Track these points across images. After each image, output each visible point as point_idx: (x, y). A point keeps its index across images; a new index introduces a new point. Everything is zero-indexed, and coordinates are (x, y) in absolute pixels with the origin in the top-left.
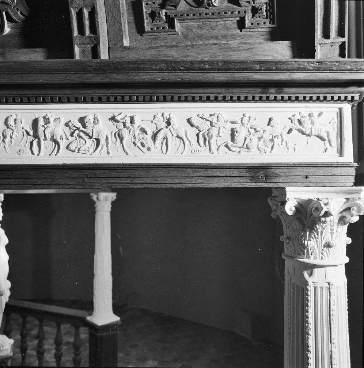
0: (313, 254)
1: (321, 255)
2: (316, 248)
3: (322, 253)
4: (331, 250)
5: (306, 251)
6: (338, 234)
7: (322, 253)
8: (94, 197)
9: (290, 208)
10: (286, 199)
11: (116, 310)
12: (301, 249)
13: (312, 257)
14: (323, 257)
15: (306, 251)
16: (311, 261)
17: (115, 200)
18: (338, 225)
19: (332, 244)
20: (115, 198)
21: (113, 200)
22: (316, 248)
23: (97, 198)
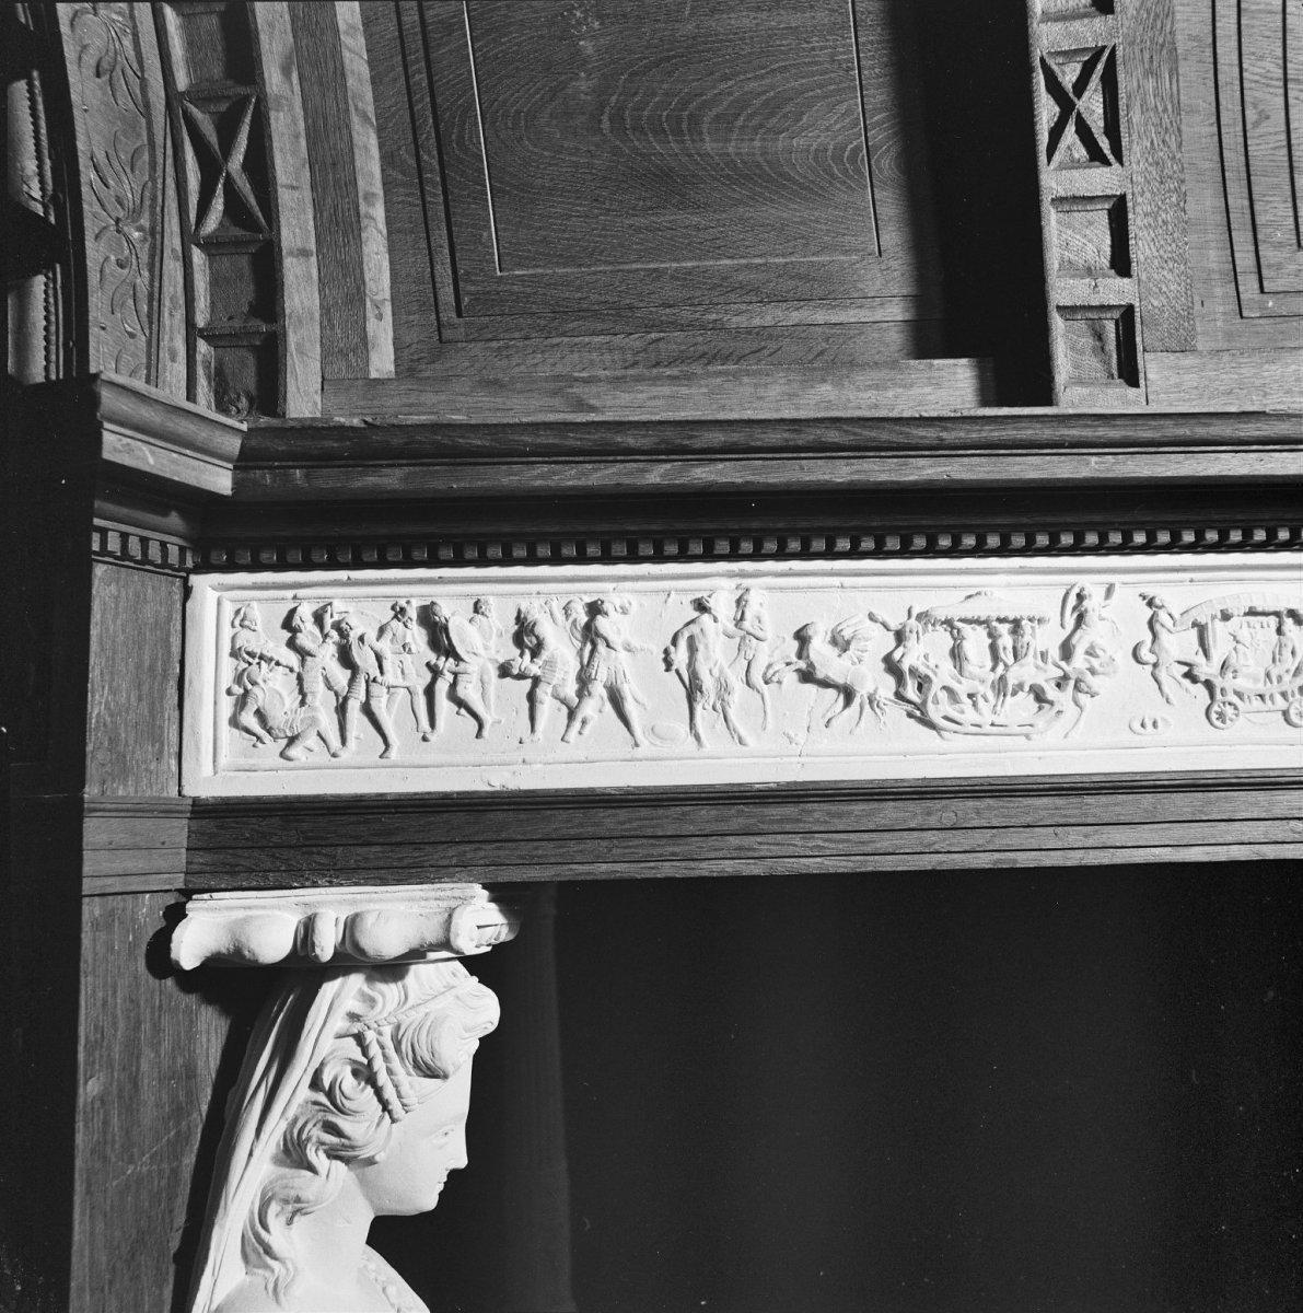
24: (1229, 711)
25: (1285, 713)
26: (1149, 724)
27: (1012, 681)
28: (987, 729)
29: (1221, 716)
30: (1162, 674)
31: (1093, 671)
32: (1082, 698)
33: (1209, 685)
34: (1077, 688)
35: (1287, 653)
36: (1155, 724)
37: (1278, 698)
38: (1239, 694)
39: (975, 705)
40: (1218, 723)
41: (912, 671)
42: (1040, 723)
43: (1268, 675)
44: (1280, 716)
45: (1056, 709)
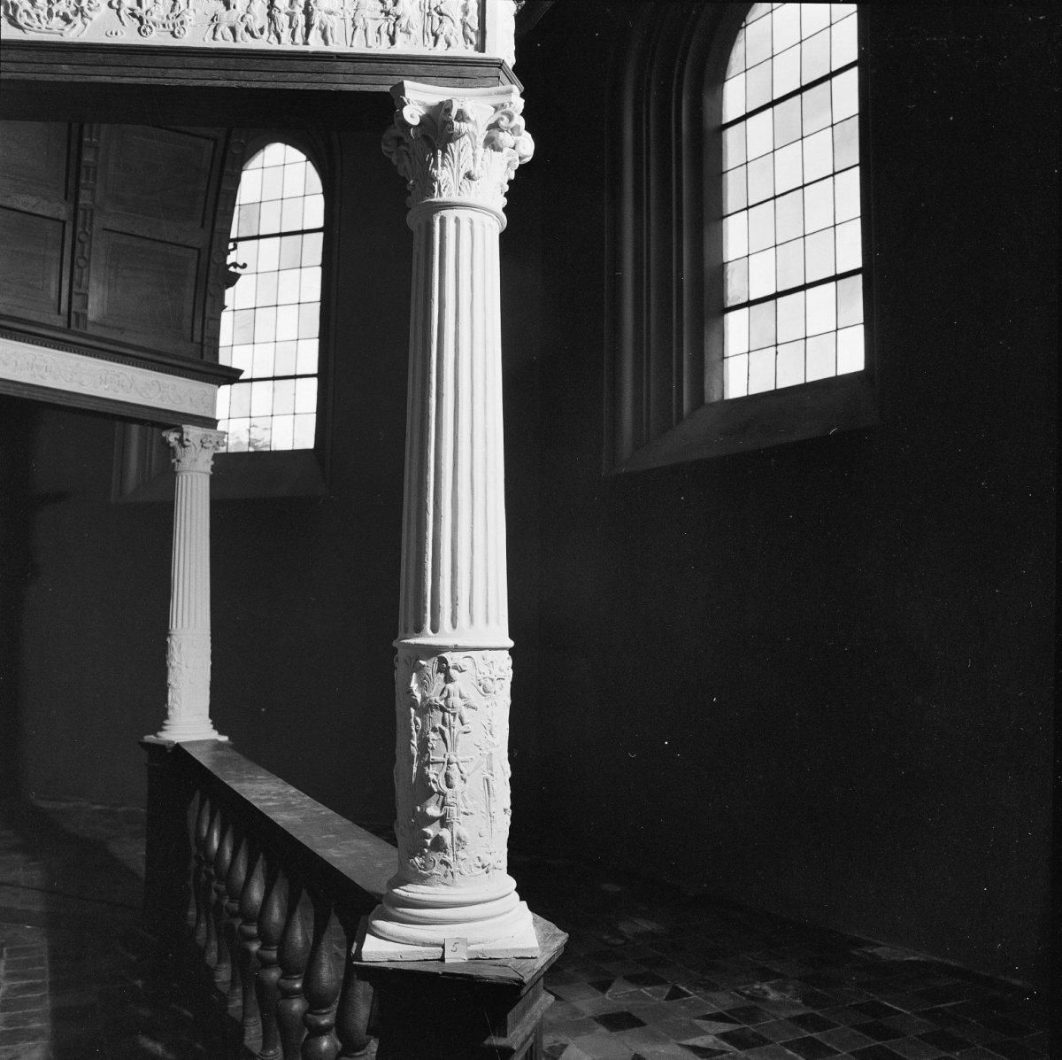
1: (458, 191)
2: (451, 180)
5: (436, 186)
6: (484, 163)
8: (172, 437)
9: (412, 114)
10: (405, 100)
11: (219, 715)
12: (428, 182)
13: (444, 194)
14: (461, 193)
16: (445, 198)
18: (485, 147)
22: (451, 180)
23: (181, 441)
24: (148, 30)
25: (173, 33)
26: (114, 33)
27: (54, 11)
28: (44, 29)
29: (144, 31)
30: (122, 13)
31: (90, 9)
32: (86, 19)
33: (141, 19)
34: (83, 16)
35: (177, 8)
36: (116, 34)
37: (171, 26)
38: (154, 24)
39: (39, 21)
40: (145, 35)
41: (12, 3)
42: (67, 28)
43: (168, 17)
44: (169, 33)
45: (72, 24)
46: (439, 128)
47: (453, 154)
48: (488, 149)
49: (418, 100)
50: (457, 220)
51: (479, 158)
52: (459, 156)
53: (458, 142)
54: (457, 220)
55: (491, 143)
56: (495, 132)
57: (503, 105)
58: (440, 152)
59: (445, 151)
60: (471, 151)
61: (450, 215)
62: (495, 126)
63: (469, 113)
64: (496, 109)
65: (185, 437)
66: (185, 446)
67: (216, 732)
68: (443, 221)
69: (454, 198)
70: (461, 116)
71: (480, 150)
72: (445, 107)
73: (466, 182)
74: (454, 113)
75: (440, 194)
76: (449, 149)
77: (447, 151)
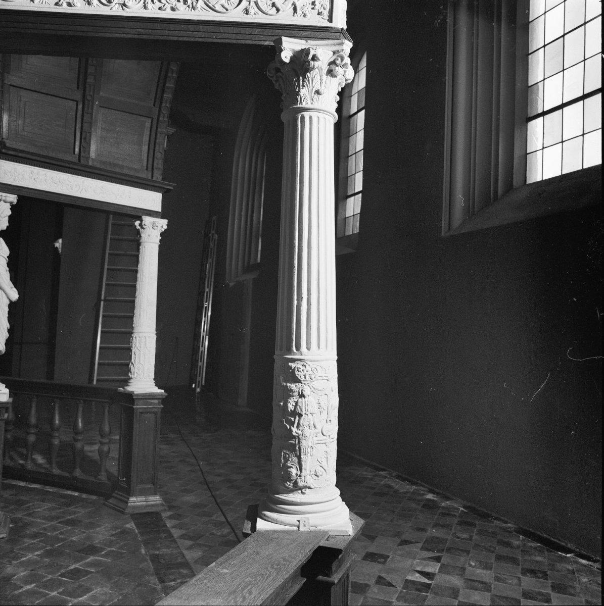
0: (305, 100)
2: (307, 94)
3: (312, 99)
4: (320, 96)
5: (299, 98)
7: (312, 99)
9: (286, 56)
10: (283, 48)
13: (304, 103)
14: (313, 103)
15: (299, 98)
16: (304, 105)
17: (165, 230)
18: (327, 75)
19: (322, 92)
20: (165, 227)
21: (163, 230)
22: (307, 94)
23: (140, 225)
46: (302, 63)
47: (309, 80)
48: (329, 77)
49: (290, 47)
50: (311, 118)
51: (324, 81)
52: (313, 80)
53: (312, 72)
54: (311, 118)
55: (330, 72)
56: (333, 67)
57: (338, 51)
58: (301, 78)
59: (304, 77)
60: (319, 78)
61: (307, 115)
62: (333, 63)
63: (319, 55)
64: (334, 53)
65: (143, 224)
66: (144, 229)
67: (157, 388)
68: (303, 118)
69: (309, 106)
70: (314, 58)
71: (325, 77)
72: (306, 52)
73: (316, 96)
74: (310, 57)
75: (301, 103)
76: (307, 77)
77: (305, 78)
